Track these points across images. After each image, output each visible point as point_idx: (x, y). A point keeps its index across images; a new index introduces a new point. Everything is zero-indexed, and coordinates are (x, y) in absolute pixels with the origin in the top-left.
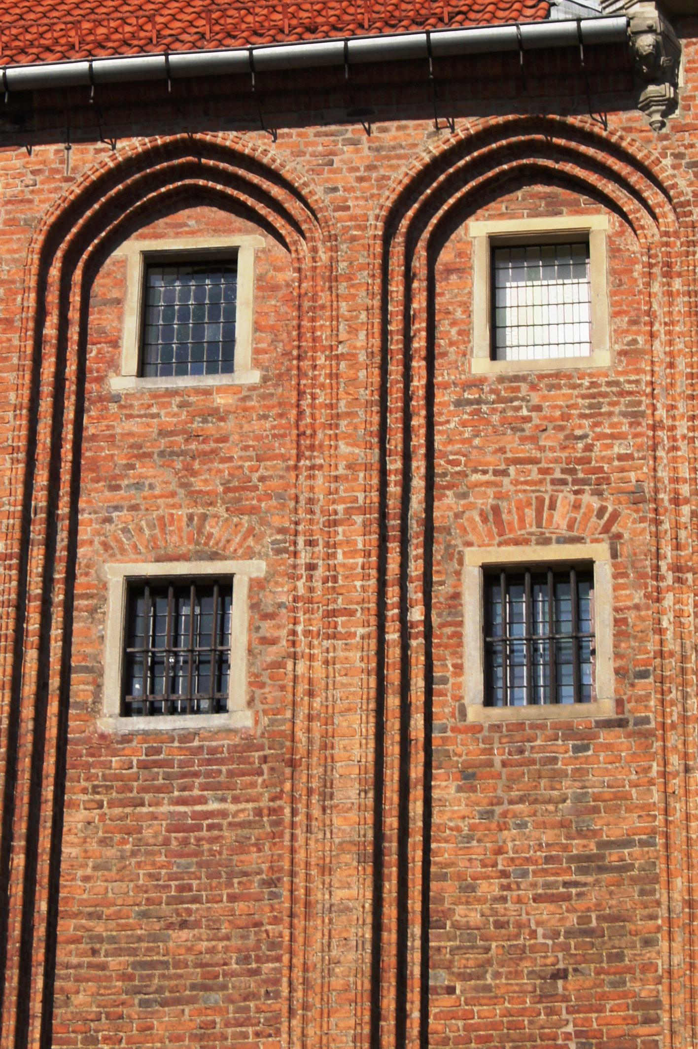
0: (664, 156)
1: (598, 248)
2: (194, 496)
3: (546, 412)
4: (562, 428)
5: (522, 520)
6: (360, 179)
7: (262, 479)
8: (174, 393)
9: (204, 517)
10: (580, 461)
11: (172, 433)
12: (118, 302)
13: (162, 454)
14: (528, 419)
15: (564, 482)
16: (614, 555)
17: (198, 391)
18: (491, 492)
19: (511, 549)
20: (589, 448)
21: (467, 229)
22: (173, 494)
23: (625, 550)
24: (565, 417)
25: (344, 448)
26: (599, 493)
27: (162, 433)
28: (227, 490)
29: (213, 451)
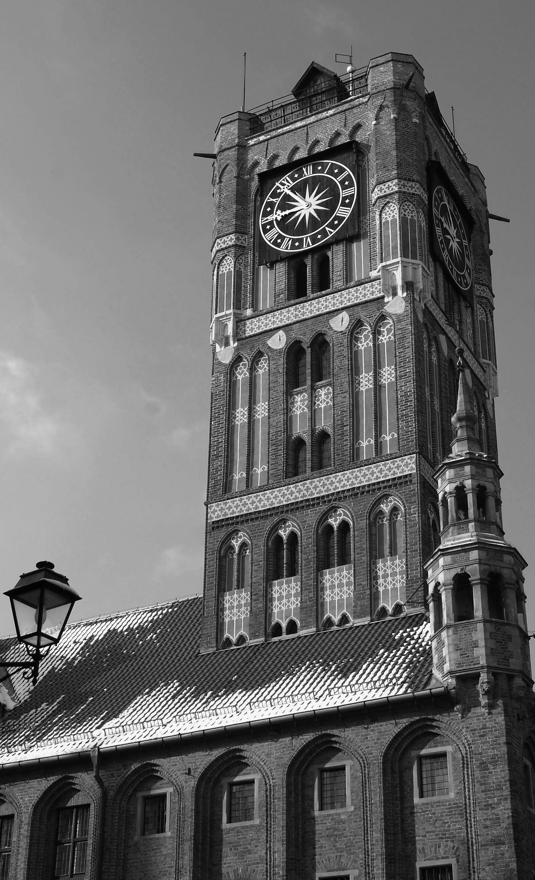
0: (463, 728)
1: (449, 758)
2: (337, 849)
3: (436, 815)
4: (441, 820)
5: (431, 851)
6: (375, 743)
7: (356, 842)
8: (329, 815)
9: (341, 856)
10: (447, 831)
11: (330, 829)
12: (313, 786)
13: (327, 836)
14: (432, 817)
15: (442, 838)
16: (458, 862)
17: (336, 814)
18: (421, 842)
19: (428, 861)
20: (449, 826)
21: (411, 754)
22: (331, 849)
23: (461, 860)
24: (442, 816)
25: (375, 834)
26: (453, 841)
27: (327, 829)
28: (346, 847)
29: (343, 834)
